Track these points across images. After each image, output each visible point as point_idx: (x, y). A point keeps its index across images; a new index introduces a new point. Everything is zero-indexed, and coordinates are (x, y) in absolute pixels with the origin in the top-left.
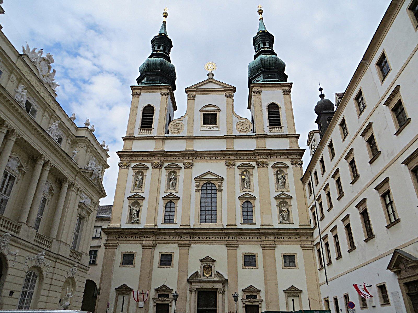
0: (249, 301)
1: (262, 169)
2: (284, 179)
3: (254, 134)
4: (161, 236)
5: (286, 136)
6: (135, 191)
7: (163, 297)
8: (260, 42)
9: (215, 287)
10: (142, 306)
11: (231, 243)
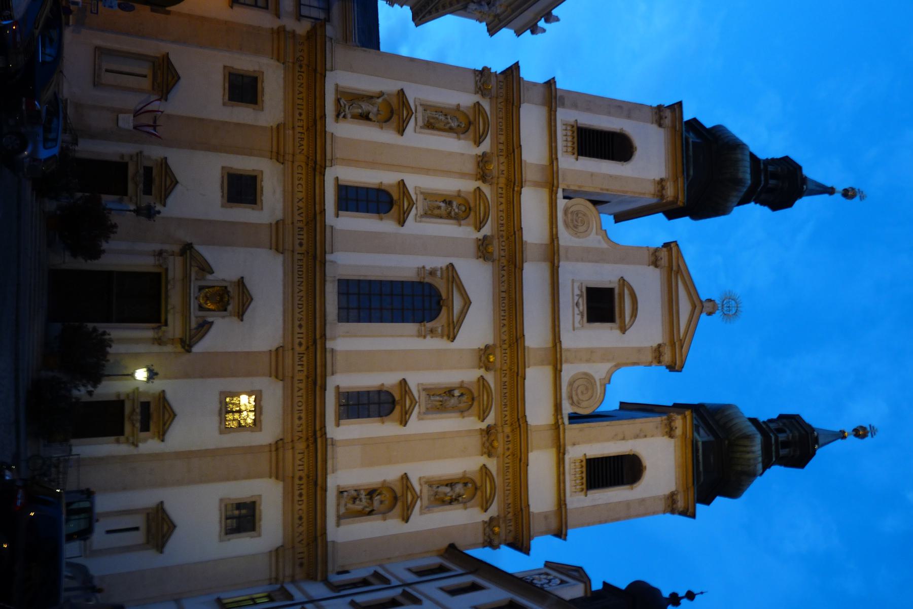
0: (134, 410)
1: (475, 442)
3: (566, 421)
4: (304, 177)
5: (561, 503)
6: (420, 109)
8: (791, 431)
10: (121, 124)
11: (288, 361)
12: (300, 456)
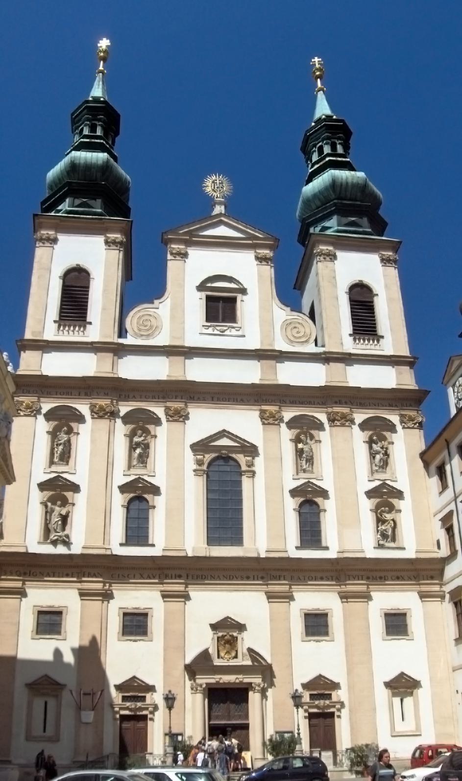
2: (386, 454)
6: (54, 468)
7: (132, 701)
9: (246, 680)
12: (351, 577)
